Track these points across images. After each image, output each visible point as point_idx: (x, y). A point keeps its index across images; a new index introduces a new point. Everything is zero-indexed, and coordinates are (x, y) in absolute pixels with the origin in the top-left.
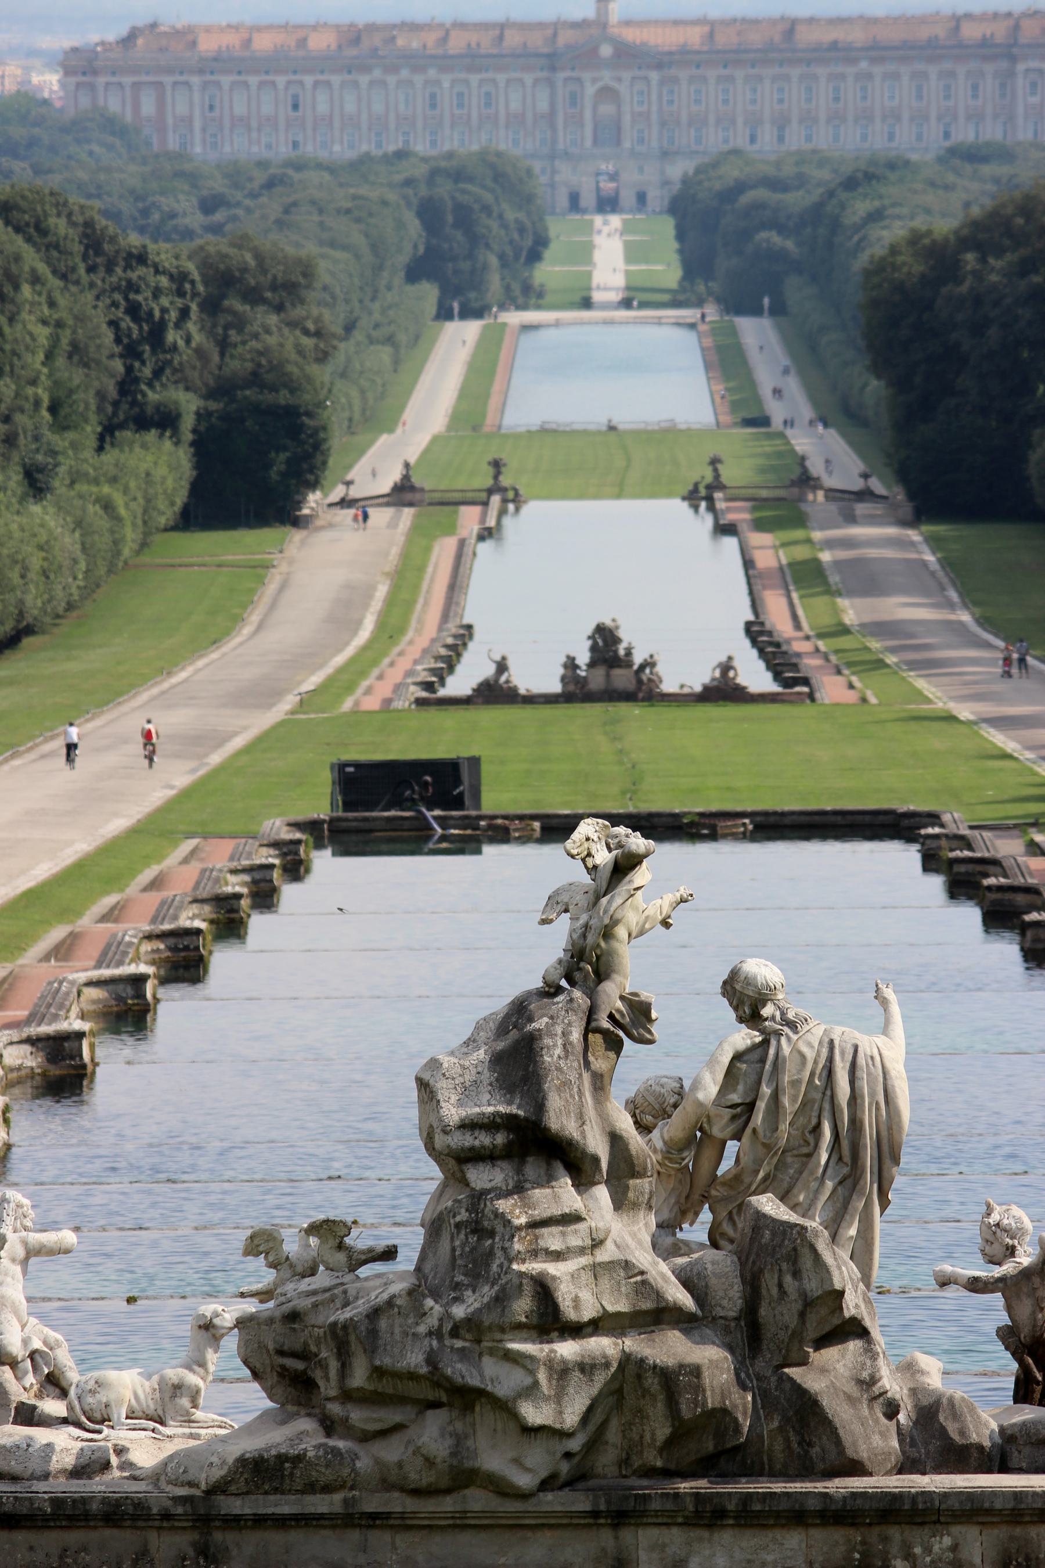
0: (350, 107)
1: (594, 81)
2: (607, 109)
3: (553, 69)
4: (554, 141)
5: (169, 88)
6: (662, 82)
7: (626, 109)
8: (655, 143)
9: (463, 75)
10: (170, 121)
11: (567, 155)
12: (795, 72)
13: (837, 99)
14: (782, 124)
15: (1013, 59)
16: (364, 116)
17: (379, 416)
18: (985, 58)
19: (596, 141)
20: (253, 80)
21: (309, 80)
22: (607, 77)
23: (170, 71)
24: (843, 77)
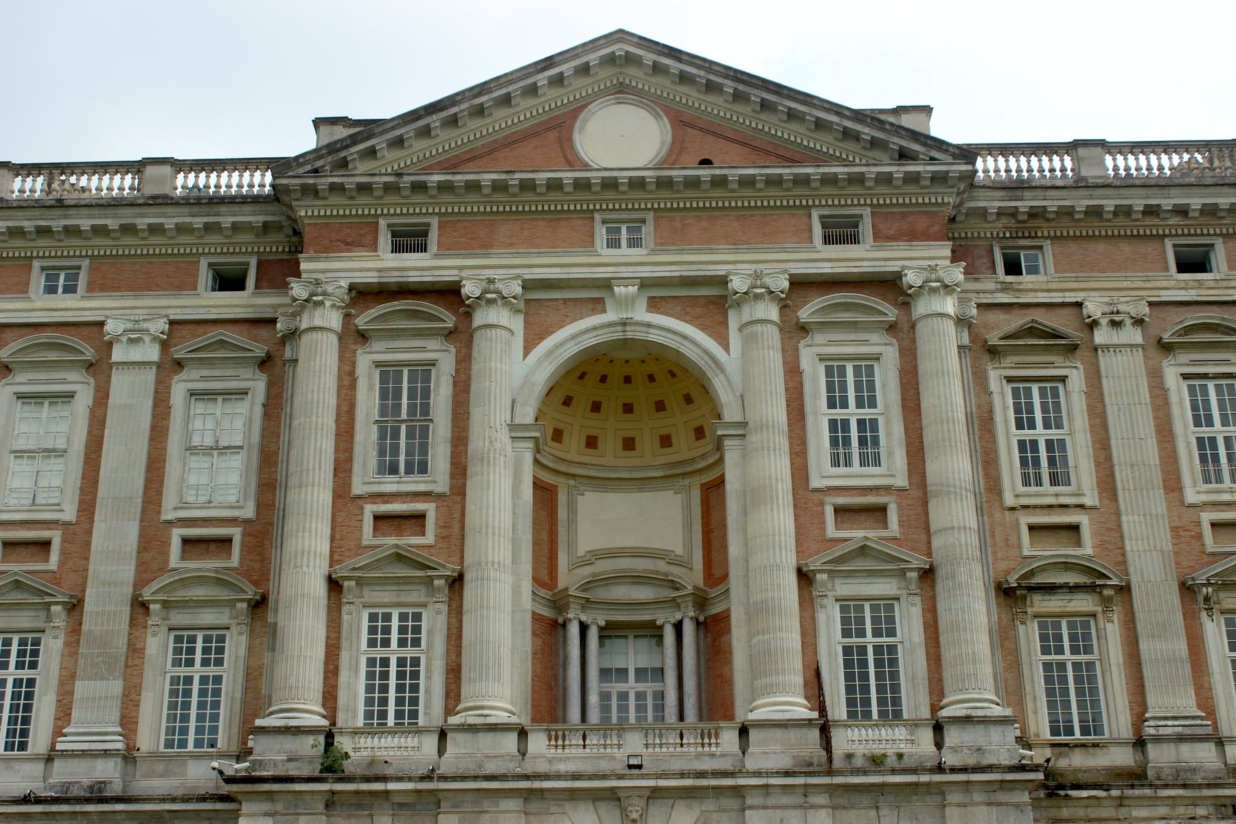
1: (543, 303)
4: (256, 697)
7: (761, 474)
8: (975, 690)
19: (548, 703)
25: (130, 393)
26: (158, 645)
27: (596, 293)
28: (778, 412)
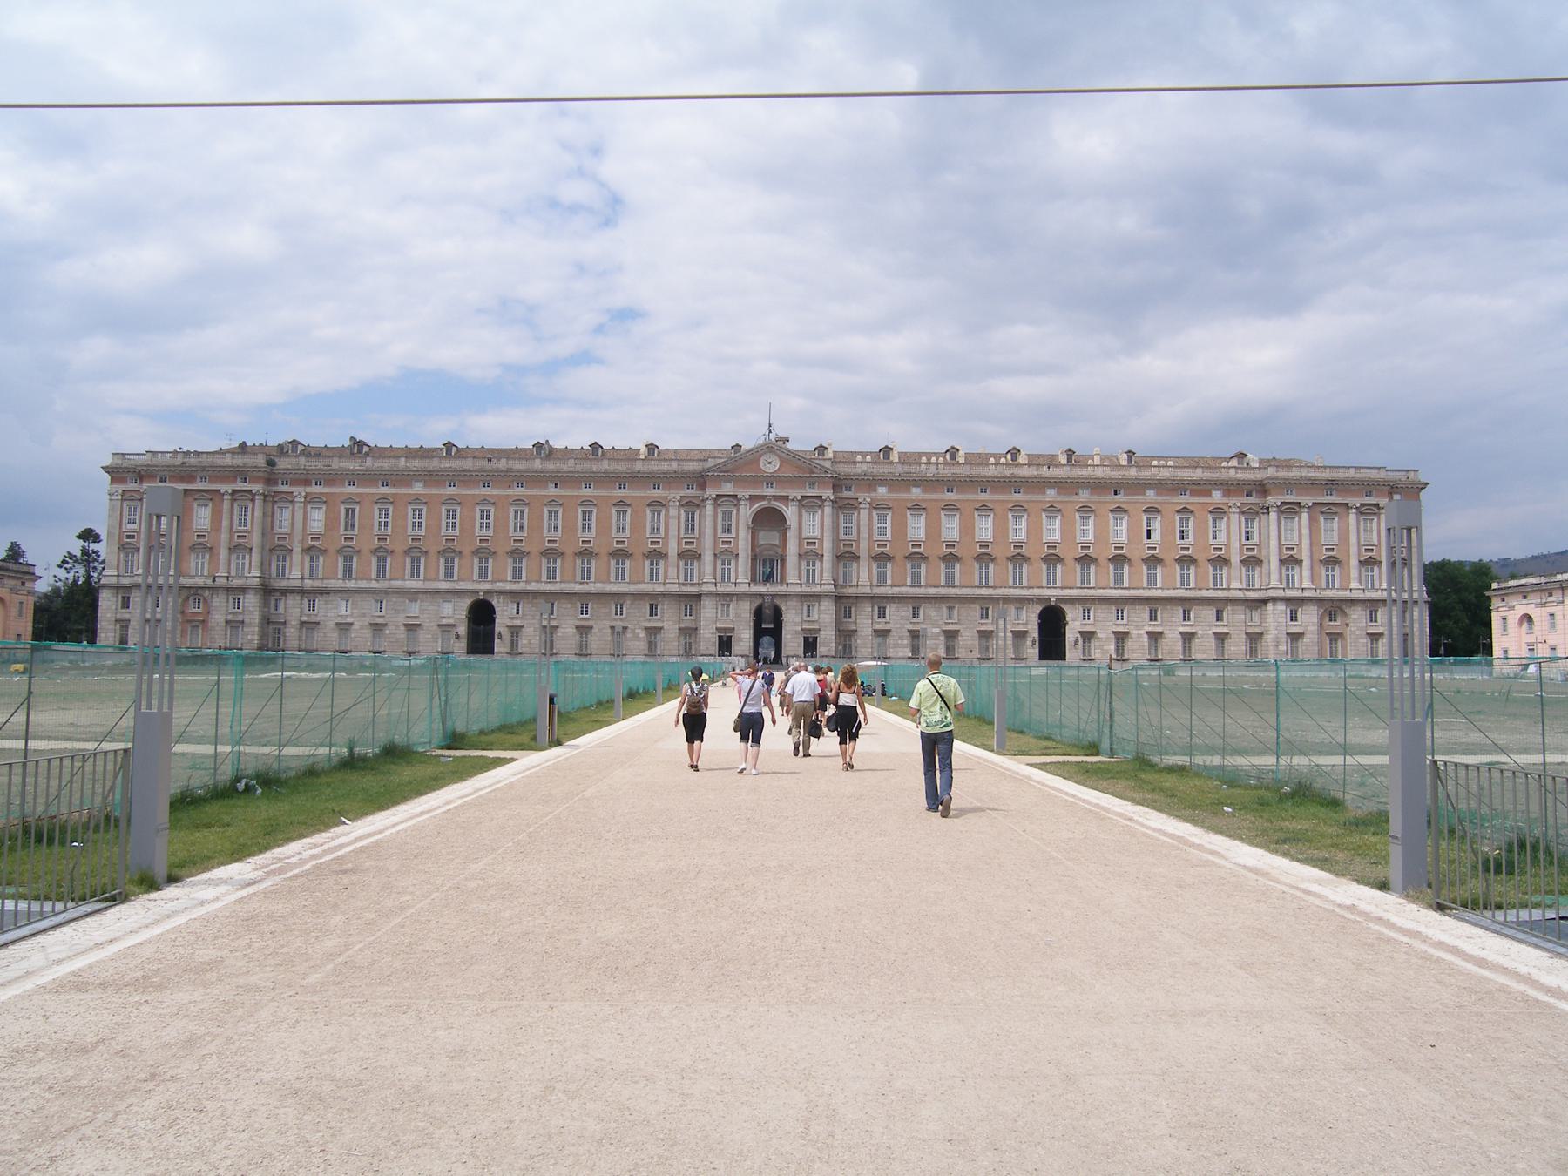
1: (753, 499)
2: (768, 537)
7: (791, 536)
27: (763, 498)
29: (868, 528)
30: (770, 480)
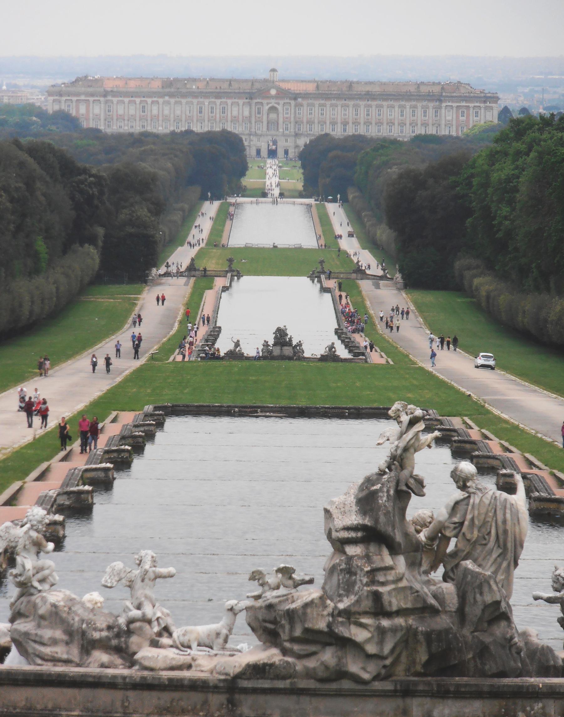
0: (166, 112)
1: (268, 104)
2: (273, 116)
3: (251, 98)
4: (250, 128)
5: (91, 102)
6: (296, 106)
7: (281, 116)
8: (292, 130)
9: (213, 100)
10: (91, 115)
11: (256, 135)
12: (351, 103)
13: (368, 115)
14: (345, 124)
15: (441, 101)
16: (172, 116)
17: (176, 239)
18: (429, 100)
19: (268, 129)
20: (126, 100)
21: (149, 100)
22: (273, 102)
23: (92, 95)
24: (370, 106)
25: (241, 107)
26: (244, 124)
28: (282, 111)
29: (304, 113)
30: (273, 97)
